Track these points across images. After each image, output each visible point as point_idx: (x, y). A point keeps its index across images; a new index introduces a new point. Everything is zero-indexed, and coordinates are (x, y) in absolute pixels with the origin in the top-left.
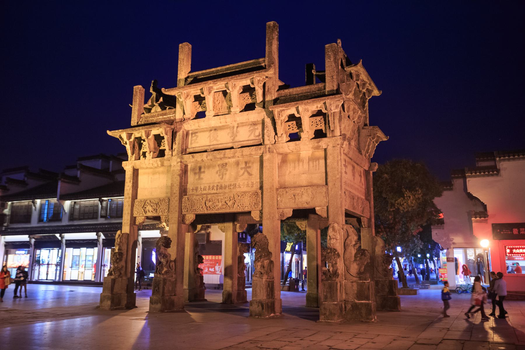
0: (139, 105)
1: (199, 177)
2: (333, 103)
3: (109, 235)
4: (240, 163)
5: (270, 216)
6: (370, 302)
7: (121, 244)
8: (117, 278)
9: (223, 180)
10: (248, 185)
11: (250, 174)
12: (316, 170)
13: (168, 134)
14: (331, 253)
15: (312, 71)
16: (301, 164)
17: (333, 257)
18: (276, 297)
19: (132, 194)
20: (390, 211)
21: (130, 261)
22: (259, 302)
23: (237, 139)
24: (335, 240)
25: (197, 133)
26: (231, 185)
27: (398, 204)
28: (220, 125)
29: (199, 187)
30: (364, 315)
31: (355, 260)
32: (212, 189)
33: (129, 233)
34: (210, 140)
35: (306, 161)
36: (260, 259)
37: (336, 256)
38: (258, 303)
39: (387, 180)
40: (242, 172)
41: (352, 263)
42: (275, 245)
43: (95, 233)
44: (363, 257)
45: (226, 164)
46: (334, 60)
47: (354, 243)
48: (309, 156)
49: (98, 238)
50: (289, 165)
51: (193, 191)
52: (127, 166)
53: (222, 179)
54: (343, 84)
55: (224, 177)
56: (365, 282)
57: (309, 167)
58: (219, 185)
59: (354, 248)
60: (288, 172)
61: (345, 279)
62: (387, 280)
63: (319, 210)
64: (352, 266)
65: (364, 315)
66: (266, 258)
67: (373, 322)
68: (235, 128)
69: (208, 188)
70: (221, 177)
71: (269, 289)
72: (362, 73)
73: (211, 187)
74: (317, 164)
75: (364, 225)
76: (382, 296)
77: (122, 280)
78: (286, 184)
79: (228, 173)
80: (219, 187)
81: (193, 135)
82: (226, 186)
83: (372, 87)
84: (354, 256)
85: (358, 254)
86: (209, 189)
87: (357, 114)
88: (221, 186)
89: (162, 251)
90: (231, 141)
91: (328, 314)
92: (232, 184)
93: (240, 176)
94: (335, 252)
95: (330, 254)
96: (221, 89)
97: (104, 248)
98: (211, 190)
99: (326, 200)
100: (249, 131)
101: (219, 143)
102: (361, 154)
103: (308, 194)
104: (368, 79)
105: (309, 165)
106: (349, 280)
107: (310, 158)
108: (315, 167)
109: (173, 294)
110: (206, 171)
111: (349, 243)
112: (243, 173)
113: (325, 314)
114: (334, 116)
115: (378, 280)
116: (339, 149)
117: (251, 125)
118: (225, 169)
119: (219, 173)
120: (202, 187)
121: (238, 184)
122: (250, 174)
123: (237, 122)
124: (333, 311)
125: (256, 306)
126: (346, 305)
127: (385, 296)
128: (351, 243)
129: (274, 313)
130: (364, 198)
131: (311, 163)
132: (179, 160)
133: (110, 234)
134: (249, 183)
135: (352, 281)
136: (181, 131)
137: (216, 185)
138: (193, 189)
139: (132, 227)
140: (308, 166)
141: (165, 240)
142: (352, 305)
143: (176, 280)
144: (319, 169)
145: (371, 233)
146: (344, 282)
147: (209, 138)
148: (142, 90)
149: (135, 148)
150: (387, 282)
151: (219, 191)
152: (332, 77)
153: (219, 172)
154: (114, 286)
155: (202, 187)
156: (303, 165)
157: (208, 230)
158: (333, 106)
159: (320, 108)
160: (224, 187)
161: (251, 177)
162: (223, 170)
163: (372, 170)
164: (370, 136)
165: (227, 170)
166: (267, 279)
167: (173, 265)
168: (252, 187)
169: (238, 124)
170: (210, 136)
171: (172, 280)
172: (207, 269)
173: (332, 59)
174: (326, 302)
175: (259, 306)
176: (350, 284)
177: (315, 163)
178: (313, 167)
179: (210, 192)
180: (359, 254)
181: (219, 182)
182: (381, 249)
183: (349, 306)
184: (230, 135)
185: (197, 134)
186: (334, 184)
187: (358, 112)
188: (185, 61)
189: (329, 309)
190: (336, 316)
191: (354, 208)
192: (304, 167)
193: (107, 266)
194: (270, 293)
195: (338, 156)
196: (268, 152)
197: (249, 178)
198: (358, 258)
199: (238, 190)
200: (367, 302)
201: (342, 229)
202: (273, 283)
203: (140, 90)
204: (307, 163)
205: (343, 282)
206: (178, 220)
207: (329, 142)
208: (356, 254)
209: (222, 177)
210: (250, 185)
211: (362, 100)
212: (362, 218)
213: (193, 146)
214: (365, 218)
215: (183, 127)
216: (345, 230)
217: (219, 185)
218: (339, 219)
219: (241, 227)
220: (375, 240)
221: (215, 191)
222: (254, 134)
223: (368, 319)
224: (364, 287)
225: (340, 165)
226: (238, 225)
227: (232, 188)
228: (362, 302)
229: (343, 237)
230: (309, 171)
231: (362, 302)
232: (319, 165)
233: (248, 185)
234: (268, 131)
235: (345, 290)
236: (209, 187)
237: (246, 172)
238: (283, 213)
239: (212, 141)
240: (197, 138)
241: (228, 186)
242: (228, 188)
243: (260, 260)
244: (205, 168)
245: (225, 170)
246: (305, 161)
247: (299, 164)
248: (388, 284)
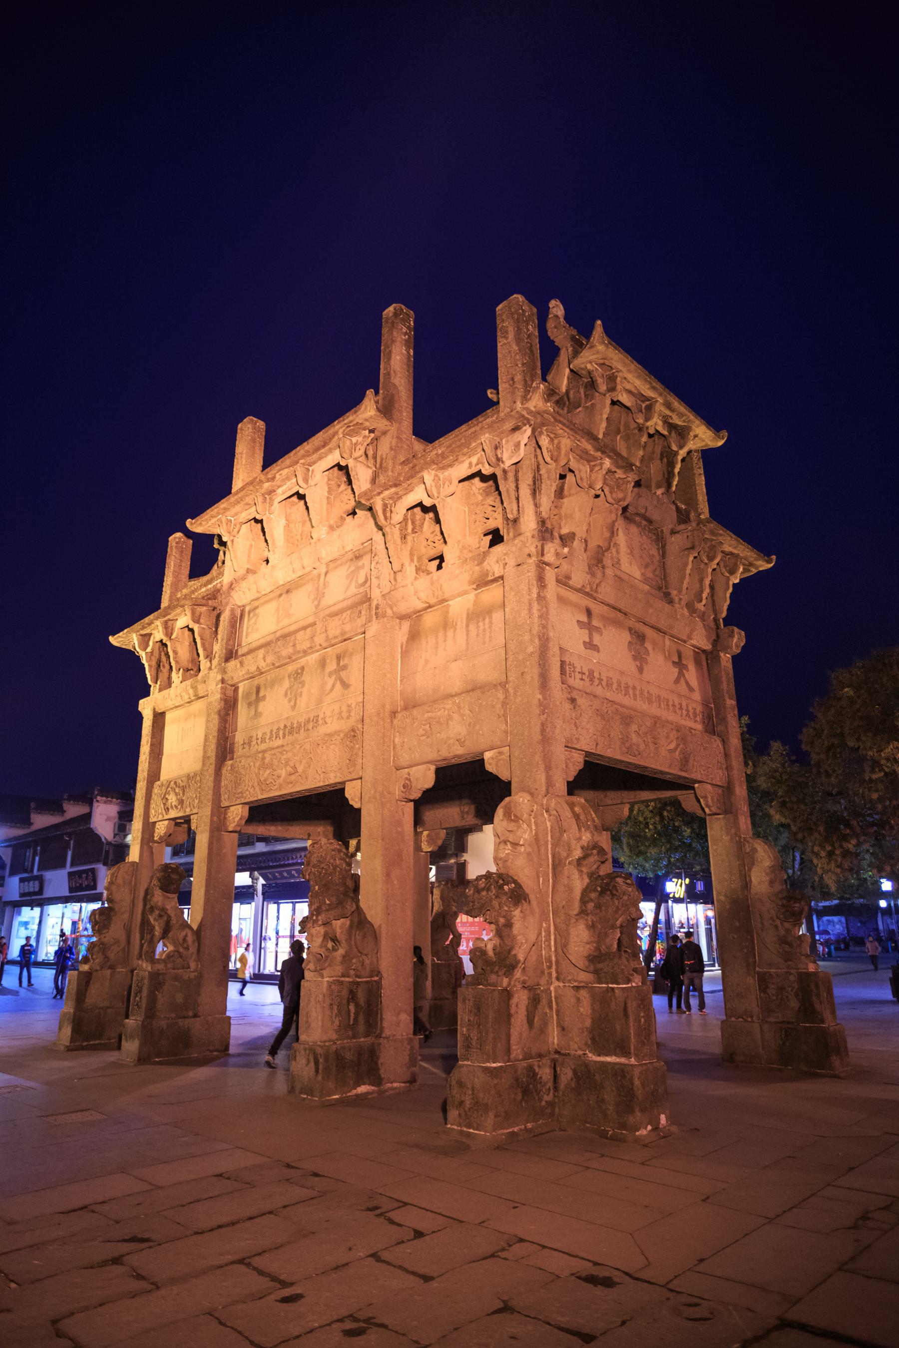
0: (173, 574)
1: (256, 711)
2: (507, 442)
3: (270, 876)
4: (328, 661)
5: (375, 792)
6: (633, 1061)
7: (114, 888)
8: (97, 971)
11: (345, 685)
12: (484, 643)
13: (202, 621)
14: (488, 890)
15: (487, 394)
16: (450, 633)
17: (495, 903)
18: (387, 1033)
19: (149, 771)
20: (871, 780)
21: (138, 927)
22: (310, 1050)
23: (326, 602)
24: (509, 846)
25: (257, 607)
26: (308, 721)
27: (888, 759)
28: (294, 576)
29: (255, 735)
30: (611, 1110)
31: (583, 912)
32: (276, 737)
33: (137, 861)
34: (278, 618)
35: (461, 624)
36: (317, 916)
37: (504, 898)
38: (307, 1052)
39: (852, 702)
40: (330, 682)
41: (573, 920)
42: (388, 875)
43: (248, 873)
44: (607, 898)
45: (303, 668)
46: (515, 336)
47: (578, 853)
48: (468, 609)
49: (252, 882)
50: (424, 642)
51: (244, 748)
52: (146, 707)
54: (578, 410)
55: (298, 702)
56: (613, 989)
57: (467, 640)
58: (289, 724)
59: (581, 871)
60: (422, 662)
61: (558, 979)
62: (793, 971)
63: (490, 761)
64: (573, 931)
65: (611, 1110)
66: (333, 913)
67: (637, 1140)
68: (322, 577)
70: (292, 703)
71: (352, 1008)
72: (620, 367)
73: (274, 733)
74: (487, 627)
75: (708, 806)
76: (783, 1022)
77: (112, 975)
78: (417, 695)
79: (305, 690)
80: (287, 730)
81: (252, 615)
83: (681, 415)
84: (578, 898)
85: (590, 892)
87: (601, 468)
89: (158, 902)
91: (468, 1104)
92: (312, 719)
93: (328, 694)
94: (501, 887)
95: (484, 893)
96: (290, 489)
97: (265, 903)
99: (503, 727)
102: (671, 602)
103: (462, 715)
104: (654, 388)
105: (467, 635)
106: (569, 981)
107: (470, 612)
108: (481, 635)
109: (191, 1013)
111: (564, 854)
112: (333, 686)
113: (461, 1103)
114: (517, 480)
115: (766, 973)
116: (533, 568)
117: (351, 560)
118: (300, 683)
120: (260, 736)
122: (345, 685)
123: (324, 561)
124: (481, 1095)
125: (304, 1061)
126: (558, 1069)
127: (788, 1023)
128: (568, 856)
129: (377, 1080)
130: (699, 727)
131: (472, 627)
132: (219, 677)
133: (270, 873)
134: (342, 709)
135: (576, 984)
136: (228, 609)
137: (282, 727)
138: (243, 744)
139: (145, 847)
140: (465, 637)
141: (162, 874)
142: (575, 1072)
143: (200, 977)
144: (490, 641)
145: (733, 831)
146: (555, 988)
148: (184, 542)
149: (162, 667)
150: (792, 978)
151: (289, 738)
152: (513, 379)
154: (86, 990)
155: (260, 736)
156: (454, 635)
157: (463, 856)
158: (507, 450)
159: (477, 464)
160: (297, 727)
161: (346, 692)
163: (725, 649)
164: (693, 548)
166: (343, 976)
167: (186, 936)
168: (348, 718)
169: (327, 565)
170: (278, 609)
171: (186, 977)
172: (465, 944)
173: (511, 336)
174: (468, 1059)
175: (308, 1061)
176: (570, 993)
177: (481, 624)
178: (477, 636)
180: (595, 890)
181: (288, 718)
182: (767, 874)
183: (566, 1075)
184: (313, 597)
185: (257, 611)
186: (522, 674)
187: (601, 464)
188: (244, 456)
189: (473, 1089)
190: (491, 1115)
191: (629, 750)
192: (456, 641)
193: (270, 939)
194: (361, 1021)
195: (529, 588)
196: (374, 617)
198: (591, 906)
199: (322, 730)
200: (623, 1060)
201: (547, 811)
202: (374, 992)
203: (177, 543)
204: (464, 630)
205: (552, 988)
206: (212, 821)
207: (505, 554)
208: (585, 892)
210: (345, 715)
211: (665, 460)
212: (696, 785)
213: (250, 640)
214: (709, 786)
215: (231, 600)
216: (555, 812)
218: (535, 781)
219: (430, 840)
220: (748, 850)
222: (356, 581)
223: (623, 1126)
224: (613, 1005)
225: (536, 613)
226: (425, 833)
227: (310, 727)
228: (609, 1059)
229: (549, 838)
230: (467, 649)
231: (609, 1059)
232: (490, 627)
233: (340, 717)
234: (377, 563)
235: (557, 1015)
237: (338, 682)
238: (410, 780)
240: (256, 621)
243: (317, 920)
244: (266, 688)
245: (300, 686)
246: (459, 624)
247: (446, 636)
248: (796, 985)
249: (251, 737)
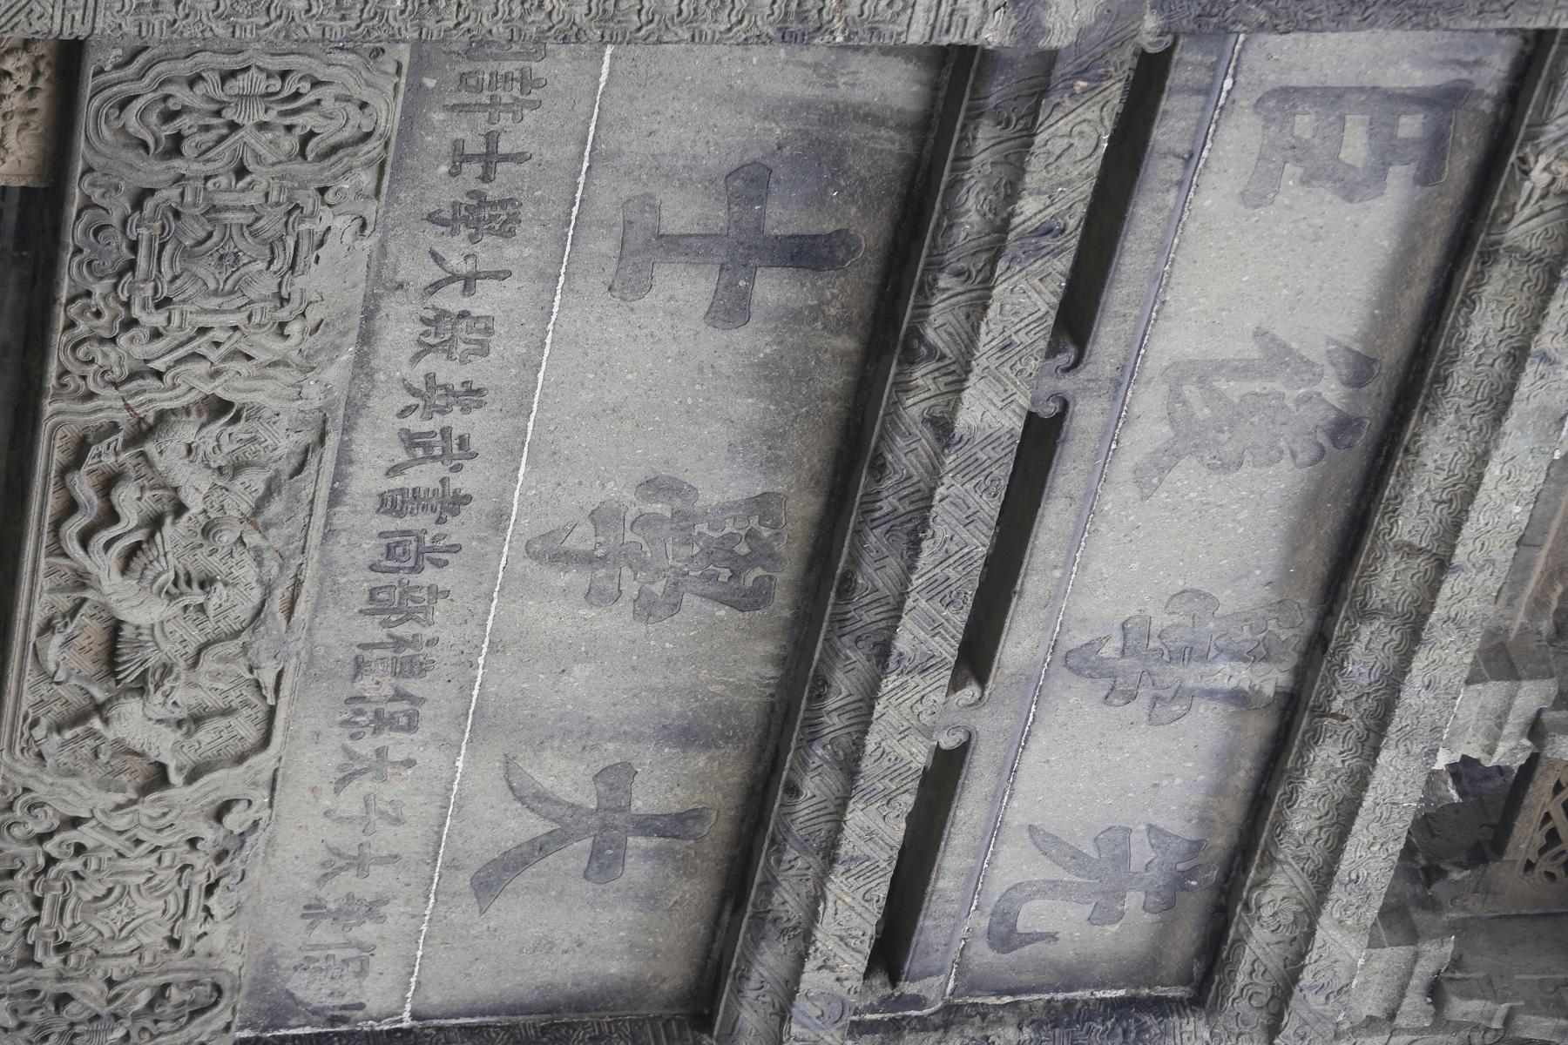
1: (671, 245)
9: (525, 565)
10: (359, 863)
32: (411, 440)
34: (1204, 372)
51: (460, 157)
53: (535, 556)
69: (450, 372)
70: (582, 539)
81: (1411, 125)
82: (408, 617)
86: (431, 395)
88: (427, 554)
90: (1077, 638)
92: (413, 686)
93: (508, 761)
98: (414, 423)
100: (1116, 841)
101: (1117, 498)
110: (742, 337)
119: (635, 506)
121: (396, 755)
137: (460, 482)
138: (490, 158)
147: (1252, 351)
153: (660, 508)
155: (487, 300)
160: (407, 590)
161: (463, 881)
162: (673, 555)
165: (646, 608)
179: (385, 406)
185: (1399, 179)
197: (453, 866)
209: (561, 558)
217: (456, 529)
221: (367, 480)
222: (1051, 888)
236: (472, 395)
237: (538, 827)
239: (1190, 391)
241: (399, 643)
242: (380, 635)
245: (658, 588)
249: (506, 230)
